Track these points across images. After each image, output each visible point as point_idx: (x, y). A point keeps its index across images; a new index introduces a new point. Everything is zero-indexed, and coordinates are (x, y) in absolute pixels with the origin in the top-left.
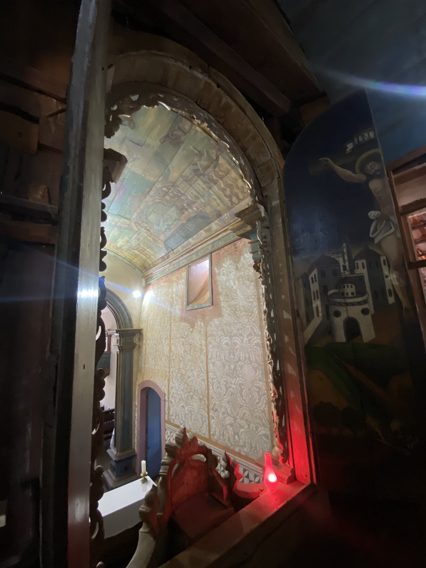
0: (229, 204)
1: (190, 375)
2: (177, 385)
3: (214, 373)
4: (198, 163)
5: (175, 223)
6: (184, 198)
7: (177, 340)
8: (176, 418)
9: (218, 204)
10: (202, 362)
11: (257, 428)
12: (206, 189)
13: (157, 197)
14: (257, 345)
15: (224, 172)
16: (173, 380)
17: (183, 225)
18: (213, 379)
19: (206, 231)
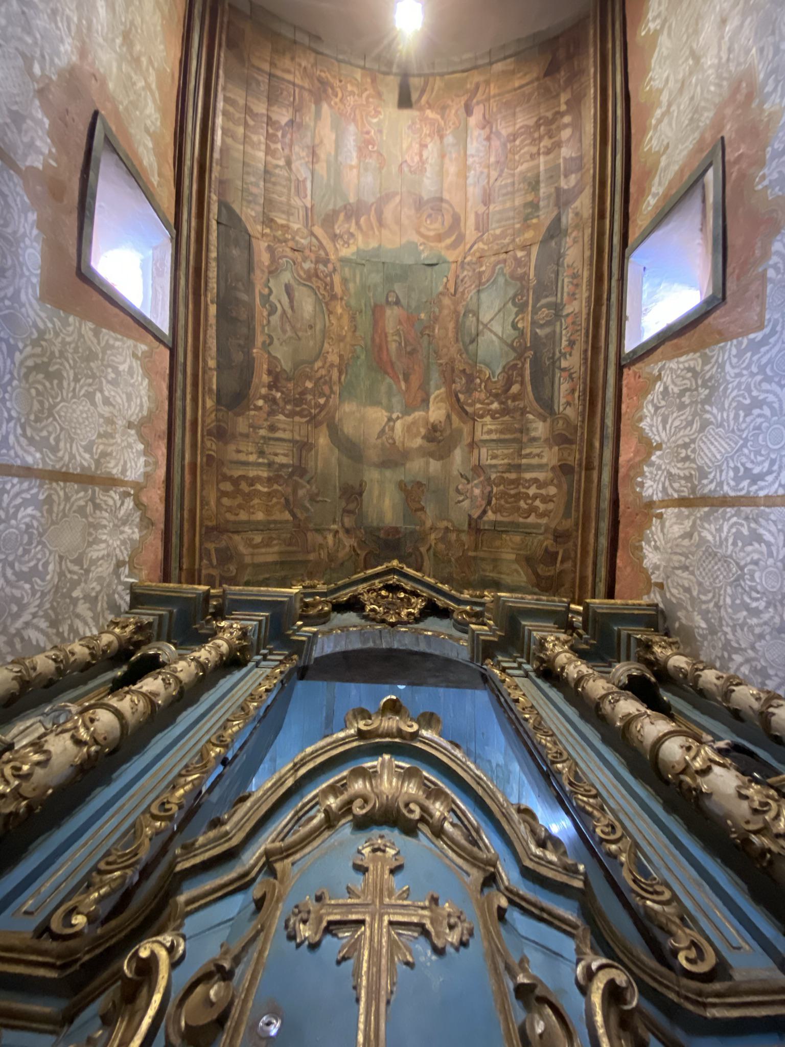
4: (308, 487)
6: (288, 407)
12: (272, 457)
13: (323, 372)
17: (250, 339)
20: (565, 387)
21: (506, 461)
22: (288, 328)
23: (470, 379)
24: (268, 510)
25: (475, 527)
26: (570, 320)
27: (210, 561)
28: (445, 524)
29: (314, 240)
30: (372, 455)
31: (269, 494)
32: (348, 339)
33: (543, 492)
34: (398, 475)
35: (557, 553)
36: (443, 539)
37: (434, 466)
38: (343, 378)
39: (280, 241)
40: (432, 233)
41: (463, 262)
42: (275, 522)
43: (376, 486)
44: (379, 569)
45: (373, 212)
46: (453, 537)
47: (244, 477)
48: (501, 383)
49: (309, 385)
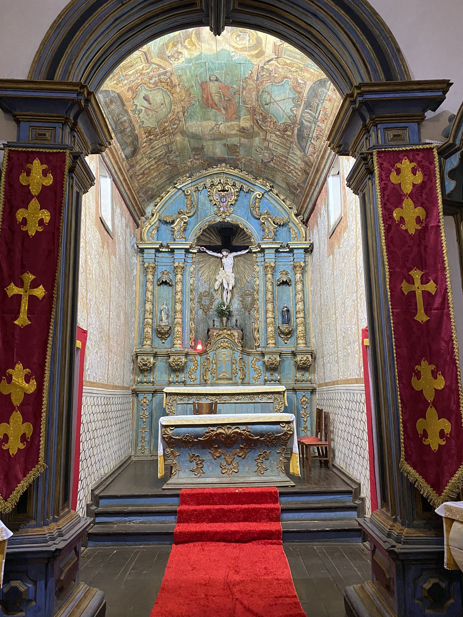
5: (139, 121)
12: (155, 156)
17: (133, 129)
22: (150, 112)
23: (264, 118)
25: (265, 164)
26: (319, 129)
29: (154, 66)
32: (186, 99)
34: (224, 142)
36: (248, 161)
38: (186, 114)
39: (133, 82)
40: (241, 47)
41: (263, 67)
43: (211, 146)
44: (216, 170)
45: (193, 35)
47: (146, 169)
48: (282, 127)
49: (166, 124)
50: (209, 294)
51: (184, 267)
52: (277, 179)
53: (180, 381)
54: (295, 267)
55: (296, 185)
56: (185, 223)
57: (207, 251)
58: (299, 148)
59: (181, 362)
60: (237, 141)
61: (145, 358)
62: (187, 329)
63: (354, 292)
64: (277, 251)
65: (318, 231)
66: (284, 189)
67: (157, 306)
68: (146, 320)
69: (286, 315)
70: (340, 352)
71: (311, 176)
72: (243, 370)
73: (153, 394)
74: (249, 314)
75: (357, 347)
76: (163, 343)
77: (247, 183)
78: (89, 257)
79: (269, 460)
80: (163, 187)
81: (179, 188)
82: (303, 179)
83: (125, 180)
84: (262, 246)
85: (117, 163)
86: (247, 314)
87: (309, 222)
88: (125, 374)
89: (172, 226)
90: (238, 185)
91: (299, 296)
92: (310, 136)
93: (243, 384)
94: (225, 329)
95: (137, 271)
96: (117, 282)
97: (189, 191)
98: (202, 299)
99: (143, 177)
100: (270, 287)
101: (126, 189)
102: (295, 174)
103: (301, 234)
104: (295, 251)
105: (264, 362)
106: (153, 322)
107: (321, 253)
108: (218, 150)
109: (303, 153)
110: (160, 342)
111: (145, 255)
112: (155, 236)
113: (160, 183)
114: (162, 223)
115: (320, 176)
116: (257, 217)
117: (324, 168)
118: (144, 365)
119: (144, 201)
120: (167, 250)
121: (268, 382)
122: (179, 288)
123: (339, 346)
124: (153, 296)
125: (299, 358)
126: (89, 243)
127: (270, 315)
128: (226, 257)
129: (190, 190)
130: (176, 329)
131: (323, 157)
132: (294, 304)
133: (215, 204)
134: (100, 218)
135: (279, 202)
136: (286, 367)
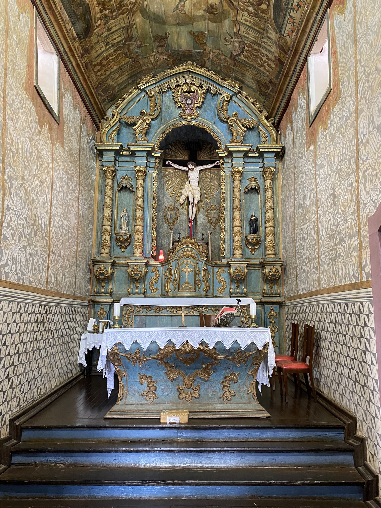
0: (95, 63)
1: (35, 198)
2: (18, 208)
3: (56, 208)
4: (135, 43)
6: (114, 14)
7: (20, 121)
8: (11, 270)
9: (97, 51)
10: (48, 188)
11: (72, 266)
14: (77, 197)
15: (119, 60)
16: (11, 193)
18: (55, 215)
19: (70, 30)
20: (289, 26)
21: (254, 39)
24: (118, 63)
25: (234, 58)
27: (101, 96)
28: (218, 51)
30: (172, 20)
31: (116, 57)
33: (269, 62)
35: (269, 88)
36: (216, 57)
37: (212, 26)
42: (122, 66)
44: (181, 69)
46: (223, 57)
47: (104, 59)
50: (175, 209)
51: (145, 172)
52: (247, 79)
53: (139, 291)
54: (265, 172)
55: (267, 81)
56: (147, 124)
57: (173, 165)
58: (274, 29)
59: (140, 271)
60: (204, 27)
61: (102, 267)
62: (148, 239)
63: (352, 173)
64: (246, 154)
65: (293, 129)
66: (254, 90)
67: (116, 213)
68: (104, 227)
69: (254, 225)
70: (323, 256)
71: (287, 63)
72: (207, 281)
73: (110, 305)
74: (215, 229)
75: (356, 243)
76: (123, 252)
77: (215, 85)
78: (10, 123)
79: (238, 384)
80: (125, 87)
81: (141, 88)
82: (276, 72)
83: (78, 65)
84: (230, 149)
85: (66, 39)
86: (212, 229)
87: (281, 125)
88: (77, 282)
89: (134, 128)
90: (205, 86)
91: (269, 204)
92: (290, 6)
93: (207, 296)
94: (187, 237)
95: (95, 177)
96: (64, 176)
97: (153, 92)
98: (167, 213)
99: (101, 69)
100: (237, 194)
101: (81, 79)
102: (267, 68)
103: (272, 138)
104: (266, 155)
105: (230, 274)
106: (111, 229)
107: (297, 150)
108: (183, 40)
109: (278, 34)
110: (120, 251)
111: (104, 158)
112: (115, 138)
113: (121, 81)
114: (124, 126)
115: (298, 61)
116: (225, 120)
117: (304, 47)
118: (102, 274)
119: (104, 101)
120: (128, 154)
121: (234, 295)
122: (140, 193)
123: (322, 248)
124: (112, 202)
125: (267, 270)
126: (11, 105)
127: (237, 223)
128: (192, 171)
129: (154, 91)
130: (137, 236)
131: (304, 31)
132: (263, 213)
133: (180, 107)
134: (35, 87)
135: (248, 105)
136: (253, 279)
